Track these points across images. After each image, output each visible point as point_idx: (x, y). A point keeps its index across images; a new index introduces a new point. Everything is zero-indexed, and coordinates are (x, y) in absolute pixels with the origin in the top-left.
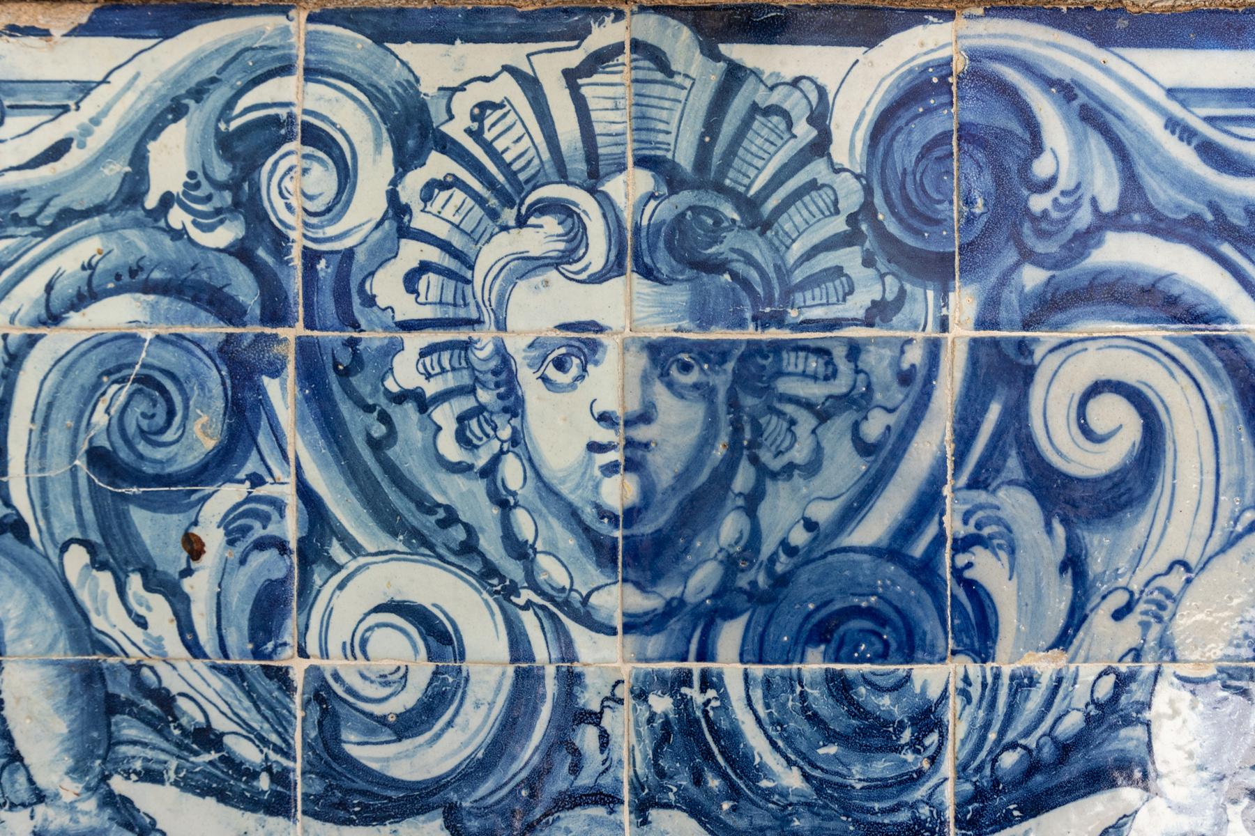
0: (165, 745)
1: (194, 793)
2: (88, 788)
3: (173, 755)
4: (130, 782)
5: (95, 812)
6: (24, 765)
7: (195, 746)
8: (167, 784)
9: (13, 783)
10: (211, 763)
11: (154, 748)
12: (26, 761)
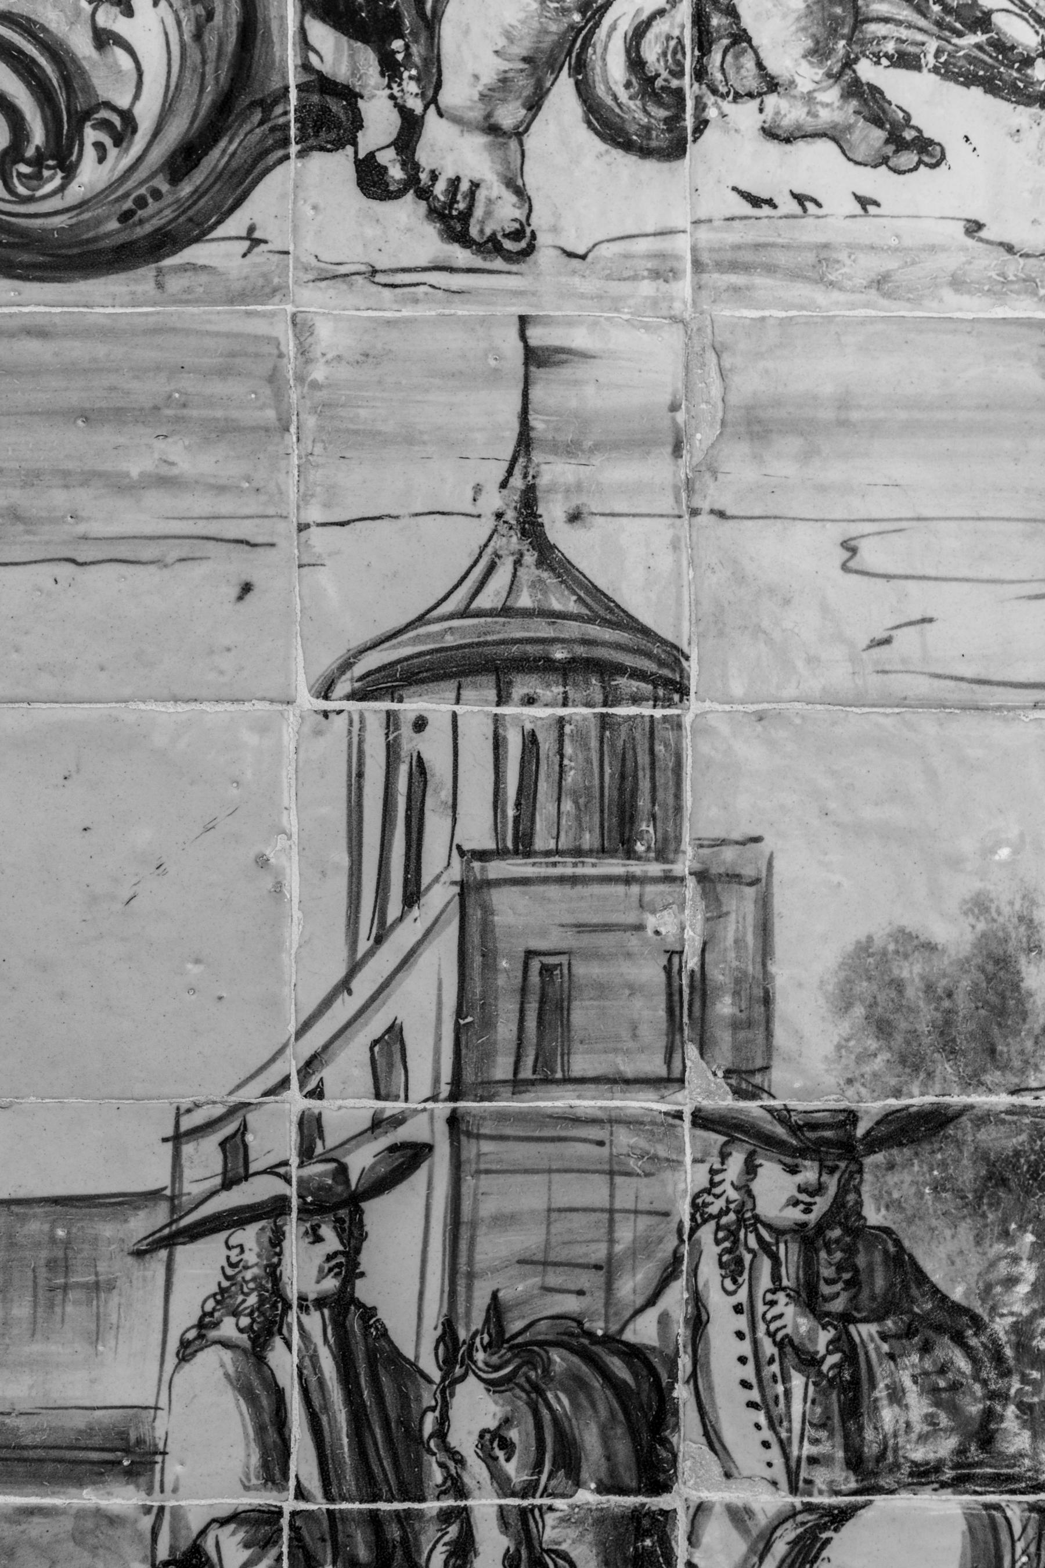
0: (922, 22)
1: (957, 82)
2: (829, 75)
3: (931, 35)
4: (880, 67)
5: (837, 104)
6: (751, 47)
7: (958, 25)
8: (925, 70)
9: (739, 68)
10: (979, 47)
11: (910, 26)
12: (754, 43)
